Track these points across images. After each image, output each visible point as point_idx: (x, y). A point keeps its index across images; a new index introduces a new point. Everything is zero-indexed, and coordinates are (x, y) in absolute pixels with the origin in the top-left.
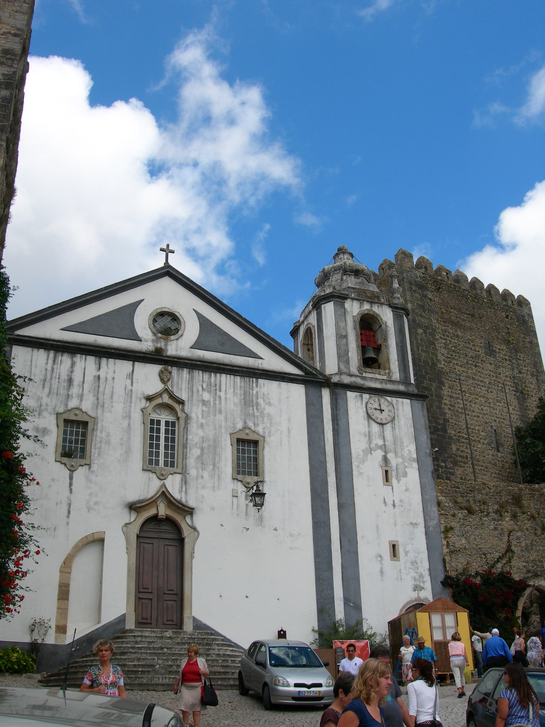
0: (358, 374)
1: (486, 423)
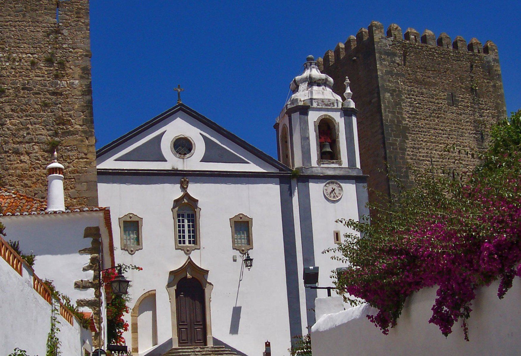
0: (317, 166)
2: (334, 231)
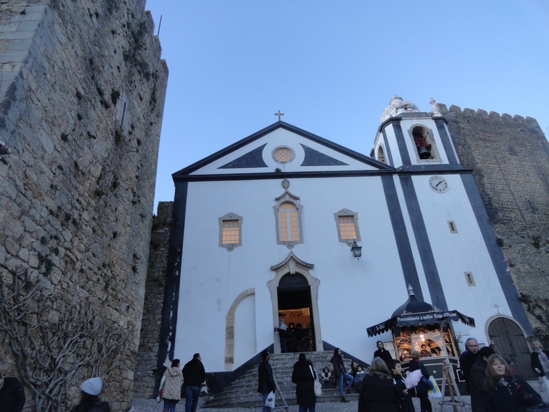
1: (521, 197)
2: (448, 222)
